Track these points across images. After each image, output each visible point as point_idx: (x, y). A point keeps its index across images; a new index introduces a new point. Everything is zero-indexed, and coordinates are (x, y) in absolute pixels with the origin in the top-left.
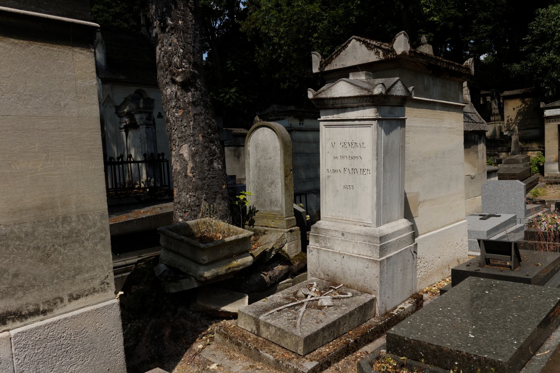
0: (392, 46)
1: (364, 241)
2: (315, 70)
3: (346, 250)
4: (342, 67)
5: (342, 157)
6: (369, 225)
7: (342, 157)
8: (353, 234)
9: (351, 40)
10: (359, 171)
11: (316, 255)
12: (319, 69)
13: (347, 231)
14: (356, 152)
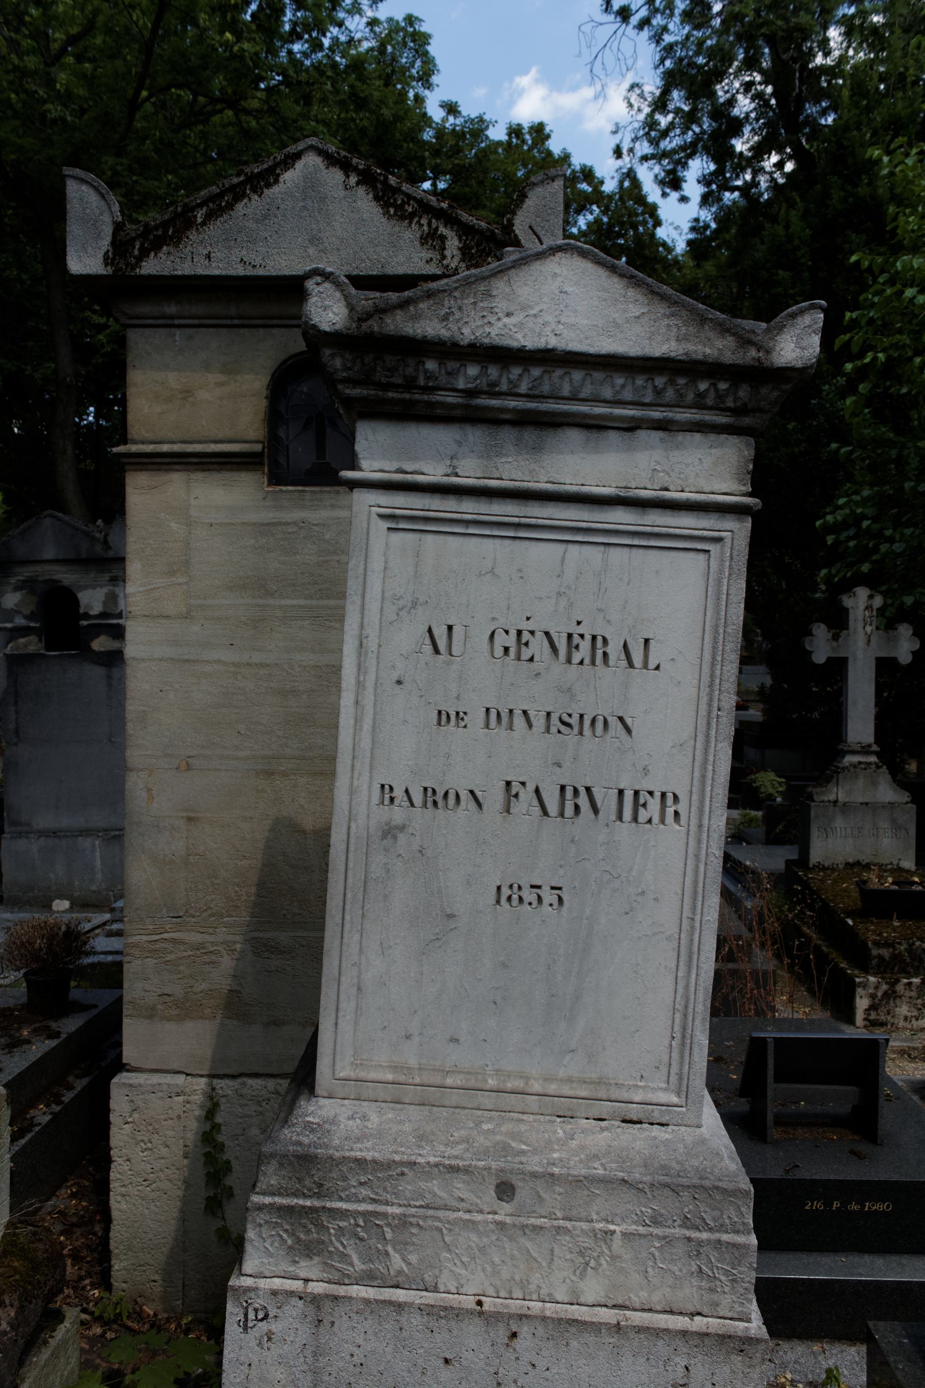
0: (511, 224)
1: (656, 1221)
2: (85, 259)
3: (524, 1284)
4: (240, 271)
5: (496, 717)
6: (657, 1115)
7: (496, 717)
8: (578, 1182)
9: (298, 156)
10: (608, 803)
11: (304, 1333)
12: (107, 261)
13: (535, 1164)
14: (599, 691)
